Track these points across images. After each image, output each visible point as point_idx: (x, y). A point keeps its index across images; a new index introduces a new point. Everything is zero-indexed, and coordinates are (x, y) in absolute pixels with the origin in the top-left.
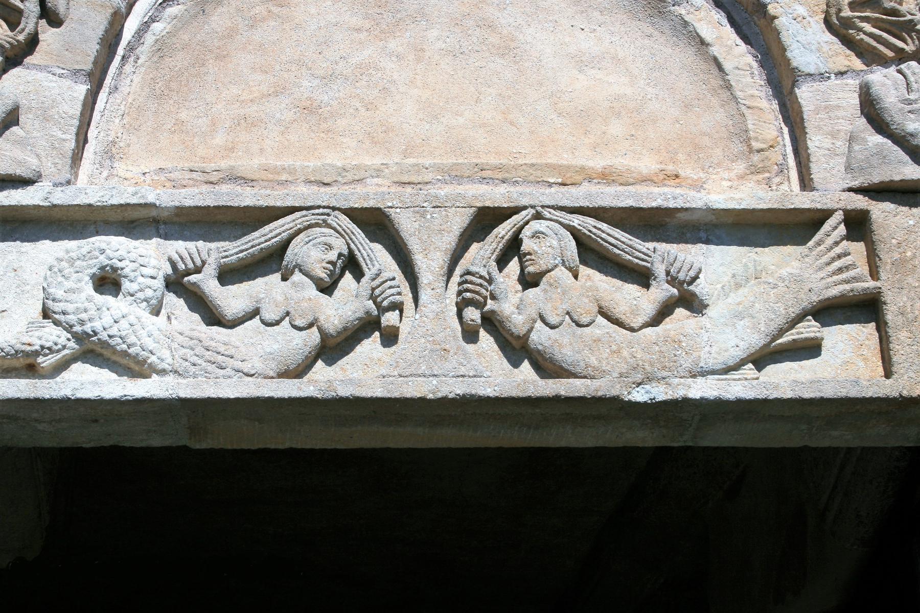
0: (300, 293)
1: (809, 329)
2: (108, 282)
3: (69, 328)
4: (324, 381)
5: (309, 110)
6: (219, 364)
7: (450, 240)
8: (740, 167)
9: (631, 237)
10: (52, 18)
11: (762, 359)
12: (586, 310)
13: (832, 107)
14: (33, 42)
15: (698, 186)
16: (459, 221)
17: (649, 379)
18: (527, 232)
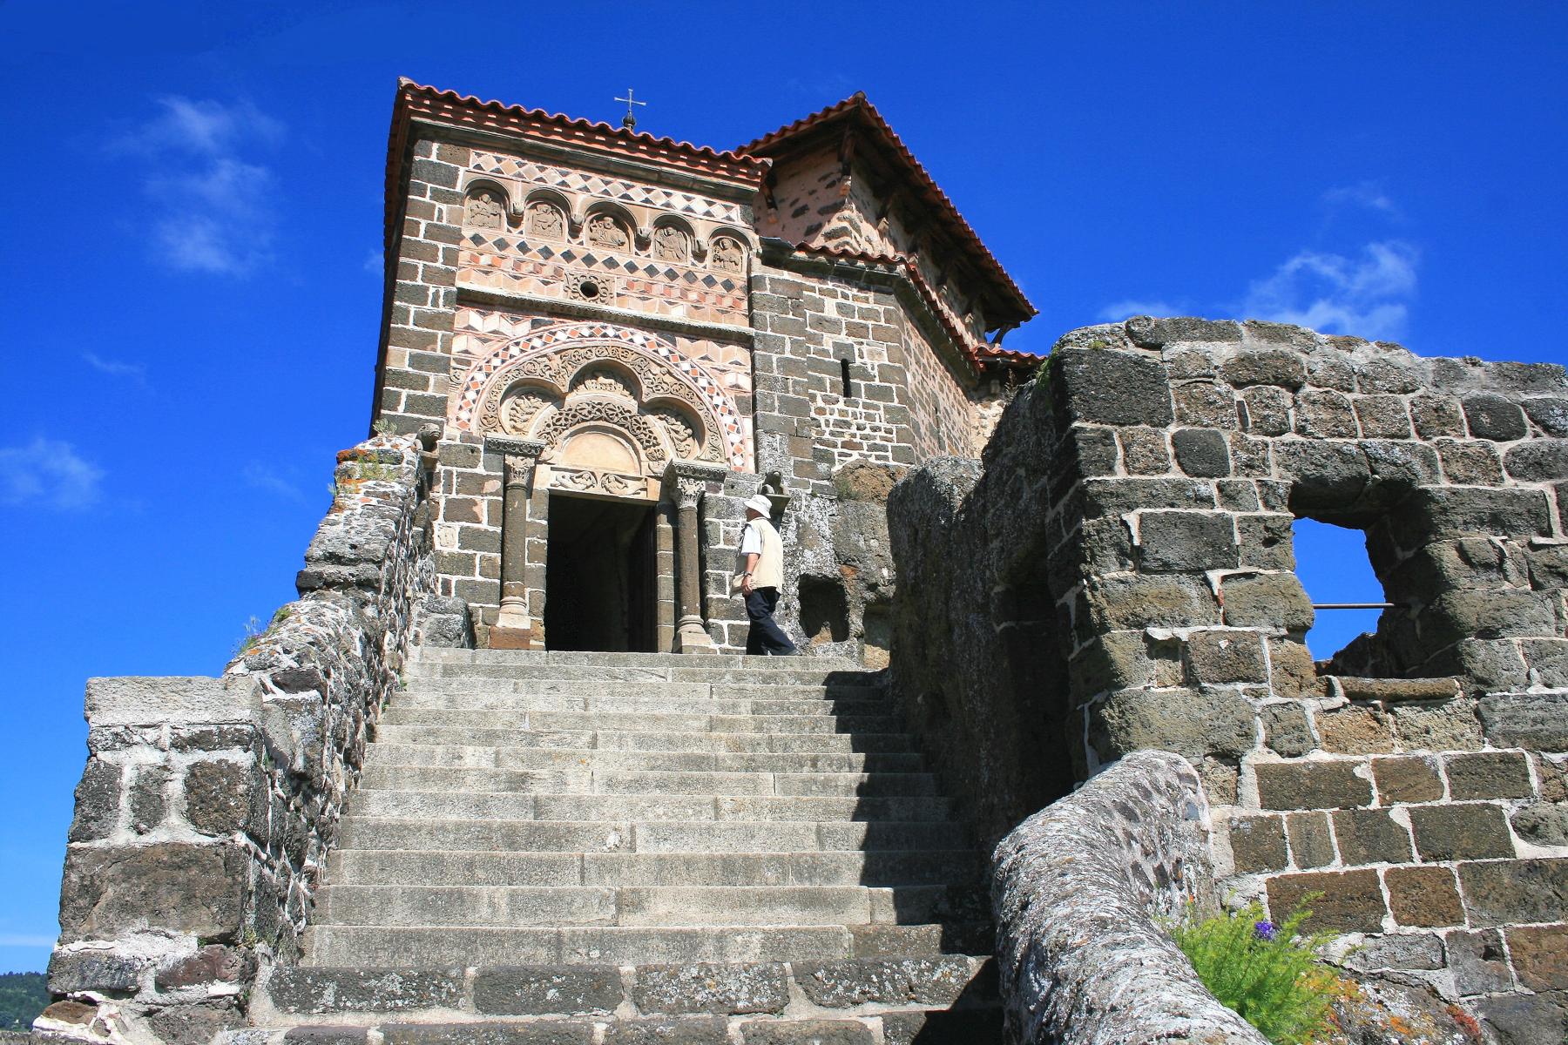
9: (621, 478)
13: (645, 465)
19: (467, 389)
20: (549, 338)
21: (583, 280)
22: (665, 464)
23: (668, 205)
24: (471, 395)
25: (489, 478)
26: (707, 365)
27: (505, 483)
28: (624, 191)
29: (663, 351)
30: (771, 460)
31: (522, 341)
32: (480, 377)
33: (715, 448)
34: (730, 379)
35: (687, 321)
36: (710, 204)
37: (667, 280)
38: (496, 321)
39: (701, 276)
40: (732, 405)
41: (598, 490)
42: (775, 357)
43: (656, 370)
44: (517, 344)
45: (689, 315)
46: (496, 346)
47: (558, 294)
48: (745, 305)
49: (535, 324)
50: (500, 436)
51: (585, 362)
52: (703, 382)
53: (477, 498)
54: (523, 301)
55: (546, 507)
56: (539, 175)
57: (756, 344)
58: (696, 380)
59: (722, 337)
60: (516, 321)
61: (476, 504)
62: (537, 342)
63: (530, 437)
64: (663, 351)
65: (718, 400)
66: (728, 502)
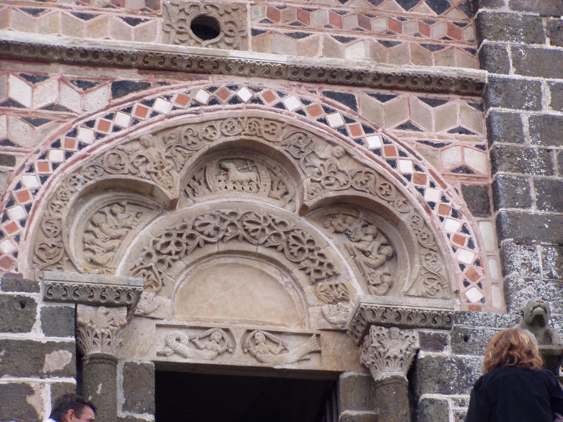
0: (213, 344)
1: (308, 357)
2: (178, 340)
3: (172, 348)
4: (219, 361)
5: (211, 305)
6: (200, 357)
7: (241, 335)
8: (297, 323)
9: (275, 336)
10: (163, 285)
11: (299, 361)
12: (267, 351)
14: (160, 290)
15: (288, 327)
16: (243, 331)
17: (278, 364)
18: (256, 335)
19: (11, 203)
22: (350, 308)
24: (17, 213)
25: (51, 347)
26: (410, 138)
27: (79, 355)
29: (335, 120)
30: (529, 290)
31: (98, 118)
32: (30, 181)
33: (433, 276)
34: (451, 157)
35: (373, 67)
38: (52, 89)
40: (457, 202)
41: (238, 359)
42: (525, 116)
43: (325, 151)
44: (90, 124)
45: (376, 55)
46: (55, 130)
48: (469, 33)
49: (119, 89)
50: (68, 276)
51: (205, 146)
52: (405, 166)
53: (33, 381)
54: (96, 53)
55: (151, 393)
57: (492, 96)
58: (393, 164)
59: (434, 88)
60: (85, 85)
61: (30, 391)
62: (122, 120)
63: (119, 274)
64: (335, 120)
65: (433, 195)
66: (460, 364)
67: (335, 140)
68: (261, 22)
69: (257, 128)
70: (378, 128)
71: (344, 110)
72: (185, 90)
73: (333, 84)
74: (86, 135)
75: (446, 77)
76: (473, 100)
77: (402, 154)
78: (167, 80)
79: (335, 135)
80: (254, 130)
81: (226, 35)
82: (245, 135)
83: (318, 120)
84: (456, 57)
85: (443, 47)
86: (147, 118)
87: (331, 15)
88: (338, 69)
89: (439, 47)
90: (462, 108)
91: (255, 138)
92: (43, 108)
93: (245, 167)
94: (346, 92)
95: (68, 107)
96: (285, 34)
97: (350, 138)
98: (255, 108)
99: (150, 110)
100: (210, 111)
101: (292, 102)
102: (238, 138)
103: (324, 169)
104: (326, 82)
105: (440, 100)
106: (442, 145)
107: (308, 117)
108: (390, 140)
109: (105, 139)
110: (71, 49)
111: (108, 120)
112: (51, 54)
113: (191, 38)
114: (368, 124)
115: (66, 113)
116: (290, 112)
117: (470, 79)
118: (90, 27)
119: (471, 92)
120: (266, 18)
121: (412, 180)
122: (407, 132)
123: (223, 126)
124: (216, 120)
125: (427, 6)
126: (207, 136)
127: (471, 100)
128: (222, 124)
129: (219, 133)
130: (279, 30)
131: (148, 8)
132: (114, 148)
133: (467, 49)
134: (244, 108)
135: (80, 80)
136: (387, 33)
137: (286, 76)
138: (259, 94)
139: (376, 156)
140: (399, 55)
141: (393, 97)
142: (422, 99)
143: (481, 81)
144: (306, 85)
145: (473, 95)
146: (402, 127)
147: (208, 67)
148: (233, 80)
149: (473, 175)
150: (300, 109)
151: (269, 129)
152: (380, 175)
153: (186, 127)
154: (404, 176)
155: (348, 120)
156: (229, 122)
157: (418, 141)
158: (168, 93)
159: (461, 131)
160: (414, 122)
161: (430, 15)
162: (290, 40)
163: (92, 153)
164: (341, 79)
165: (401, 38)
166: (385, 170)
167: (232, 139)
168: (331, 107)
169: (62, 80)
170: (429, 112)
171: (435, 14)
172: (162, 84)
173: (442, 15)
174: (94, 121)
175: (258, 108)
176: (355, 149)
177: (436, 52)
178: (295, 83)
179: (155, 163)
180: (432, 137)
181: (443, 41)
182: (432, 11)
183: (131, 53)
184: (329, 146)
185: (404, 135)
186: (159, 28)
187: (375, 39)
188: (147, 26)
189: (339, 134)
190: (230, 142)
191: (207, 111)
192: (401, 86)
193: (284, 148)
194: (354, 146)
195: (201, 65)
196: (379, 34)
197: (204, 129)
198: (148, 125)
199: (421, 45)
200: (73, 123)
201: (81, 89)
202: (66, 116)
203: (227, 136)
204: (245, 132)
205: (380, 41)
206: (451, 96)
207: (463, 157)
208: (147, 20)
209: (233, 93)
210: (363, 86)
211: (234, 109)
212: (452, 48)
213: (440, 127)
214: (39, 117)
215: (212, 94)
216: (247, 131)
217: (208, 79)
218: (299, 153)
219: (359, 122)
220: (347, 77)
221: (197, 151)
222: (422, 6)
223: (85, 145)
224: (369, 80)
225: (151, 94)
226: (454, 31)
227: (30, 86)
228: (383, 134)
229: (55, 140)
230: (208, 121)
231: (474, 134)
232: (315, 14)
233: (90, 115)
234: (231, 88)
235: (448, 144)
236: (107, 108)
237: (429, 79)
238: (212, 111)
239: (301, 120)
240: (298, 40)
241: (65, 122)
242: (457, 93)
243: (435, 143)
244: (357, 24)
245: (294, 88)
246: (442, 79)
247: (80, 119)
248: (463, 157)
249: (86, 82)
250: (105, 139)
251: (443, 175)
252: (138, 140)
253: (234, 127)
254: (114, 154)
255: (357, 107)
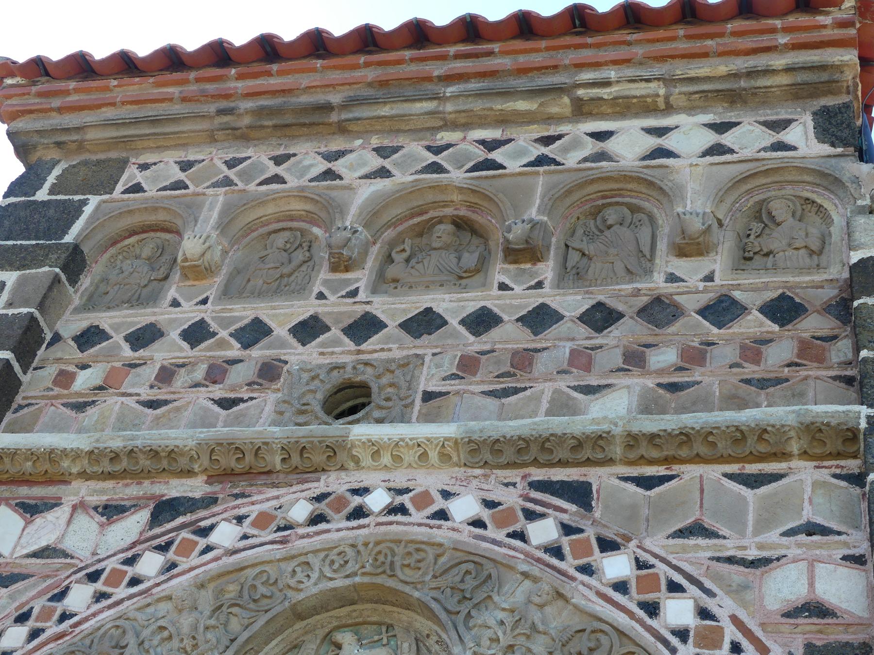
20: (186, 549)
21: (337, 378)
23: (602, 156)
26: (696, 554)
28: (480, 154)
29: (543, 532)
31: (112, 564)
34: (785, 586)
36: (721, 128)
37: (583, 330)
39: (691, 303)
44: (93, 577)
47: (264, 421)
52: (678, 611)
56: (273, 169)
58: (652, 609)
60: (111, 512)
62: (150, 564)
64: (543, 532)
67: (535, 570)
68: (444, 380)
69: (389, 558)
70: (629, 540)
71: (564, 511)
72: (275, 503)
73: (551, 465)
74: (79, 597)
75: (773, 426)
76: (842, 467)
77: (674, 588)
78: (248, 490)
79: (539, 560)
80: (383, 563)
81: (380, 408)
82: (364, 574)
83: (509, 535)
84: (811, 394)
85: (787, 380)
86: (194, 559)
87: (572, 352)
88: (552, 435)
89: (778, 381)
90: (816, 485)
91: (379, 580)
92: (28, 556)
93: (376, 638)
94: (576, 478)
95: (69, 552)
96: (483, 393)
97: (568, 565)
98: (391, 523)
99: (202, 543)
100: (308, 536)
101: (465, 507)
102: (348, 582)
103: (504, 633)
104: (536, 463)
105: (771, 475)
106: (765, 562)
107: (491, 532)
108: (652, 560)
109: (110, 601)
110: (92, 452)
111: (125, 568)
112: (65, 464)
113: (317, 418)
114: (610, 534)
115: (63, 560)
116: (456, 525)
117: (828, 425)
118: (157, 418)
119: (834, 451)
120: (455, 371)
121: (691, 640)
122: (692, 541)
123: (328, 561)
124: (316, 552)
125: (761, 316)
126: (292, 582)
127: (837, 467)
128: (327, 556)
129: (315, 576)
130: (472, 388)
131: (260, 381)
132: (120, 617)
133: (835, 378)
134: (373, 524)
135: (110, 503)
136: (675, 370)
137: (460, 460)
138: (406, 499)
139: (617, 597)
140: (694, 403)
141: (670, 478)
142: (730, 476)
143: (850, 425)
144: (498, 472)
145: (839, 455)
146: (681, 533)
147: (319, 458)
148: (363, 477)
149: (834, 621)
150: (476, 518)
151: (410, 561)
152: (621, 633)
153: (258, 570)
154: (674, 633)
155: (568, 530)
156: (339, 554)
157: (712, 559)
158: (242, 511)
159: (811, 529)
160: (709, 522)
161: (764, 329)
162: (490, 402)
163: (78, 630)
164: (563, 454)
165: (703, 374)
166: (633, 623)
167: (339, 583)
168: (539, 509)
169: (79, 507)
170: (745, 498)
171: (776, 328)
172: (236, 496)
173: (789, 327)
174: (103, 570)
175: (398, 523)
176: (574, 584)
177: (772, 389)
178: (478, 472)
179: (182, 640)
180: (744, 548)
181: (786, 369)
182: (770, 323)
183: (187, 448)
184: (527, 583)
185: (684, 549)
186: (269, 408)
187: (650, 383)
188: (247, 408)
189: (547, 557)
190: (335, 589)
191: (303, 537)
192: (684, 453)
193: (435, 594)
194: (573, 579)
195: (305, 456)
196: (660, 372)
197: (290, 569)
198: (192, 569)
199: (742, 381)
200: (68, 577)
201: (104, 519)
202: (60, 566)
203: (331, 579)
204: (364, 570)
205: (659, 385)
206: (795, 463)
207: (812, 584)
208: (252, 399)
209: (356, 500)
210: (609, 461)
211: (353, 528)
212: (806, 378)
213: (763, 525)
214: (16, 571)
215: (317, 505)
216: (368, 568)
217: (318, 480)
218: (459, 602)
219: (590, 533)
220: (574, 449)
221: (266, 611)
222: (749, 317)
223: (72, 616)
224: (618, 451)
225: (214, 516)
226: (810, 351)
227: (25, 519)
228: (638, 551)
229: (25, 609)
230: (301, 555)
231: (839, 533)
232: (545, 354)
233: (100, 561)
234: (356, 492)
235: (778, 559)
236: (134, 545)
237: (739, 435)
238: (312, 536)
239: (477, 537)
240: (503, 400)
241: (56, 576)
242: (805, 455)
243: (750, 558)
244: (621, 361)
245: (475, 482)
246: (765, 431)
247: (81, 569)
248: (812, 584)
249: (116, 507)
250: (110, 601)
251: (762, 625)
252: (169, 598)
253: (346, 562)
254: (117, 627)
255: (594, 503)
